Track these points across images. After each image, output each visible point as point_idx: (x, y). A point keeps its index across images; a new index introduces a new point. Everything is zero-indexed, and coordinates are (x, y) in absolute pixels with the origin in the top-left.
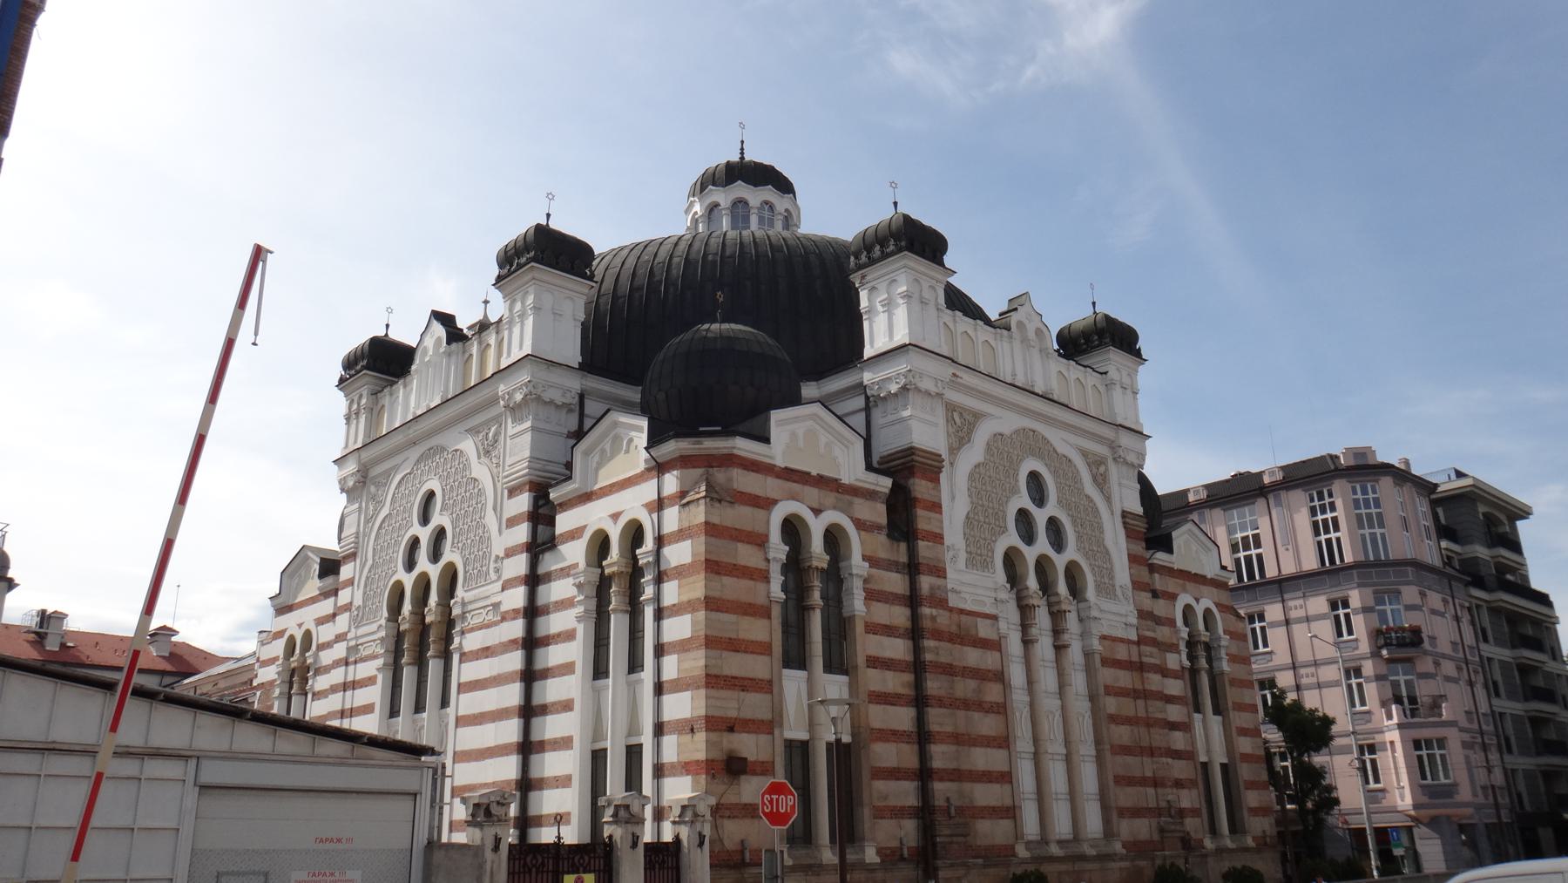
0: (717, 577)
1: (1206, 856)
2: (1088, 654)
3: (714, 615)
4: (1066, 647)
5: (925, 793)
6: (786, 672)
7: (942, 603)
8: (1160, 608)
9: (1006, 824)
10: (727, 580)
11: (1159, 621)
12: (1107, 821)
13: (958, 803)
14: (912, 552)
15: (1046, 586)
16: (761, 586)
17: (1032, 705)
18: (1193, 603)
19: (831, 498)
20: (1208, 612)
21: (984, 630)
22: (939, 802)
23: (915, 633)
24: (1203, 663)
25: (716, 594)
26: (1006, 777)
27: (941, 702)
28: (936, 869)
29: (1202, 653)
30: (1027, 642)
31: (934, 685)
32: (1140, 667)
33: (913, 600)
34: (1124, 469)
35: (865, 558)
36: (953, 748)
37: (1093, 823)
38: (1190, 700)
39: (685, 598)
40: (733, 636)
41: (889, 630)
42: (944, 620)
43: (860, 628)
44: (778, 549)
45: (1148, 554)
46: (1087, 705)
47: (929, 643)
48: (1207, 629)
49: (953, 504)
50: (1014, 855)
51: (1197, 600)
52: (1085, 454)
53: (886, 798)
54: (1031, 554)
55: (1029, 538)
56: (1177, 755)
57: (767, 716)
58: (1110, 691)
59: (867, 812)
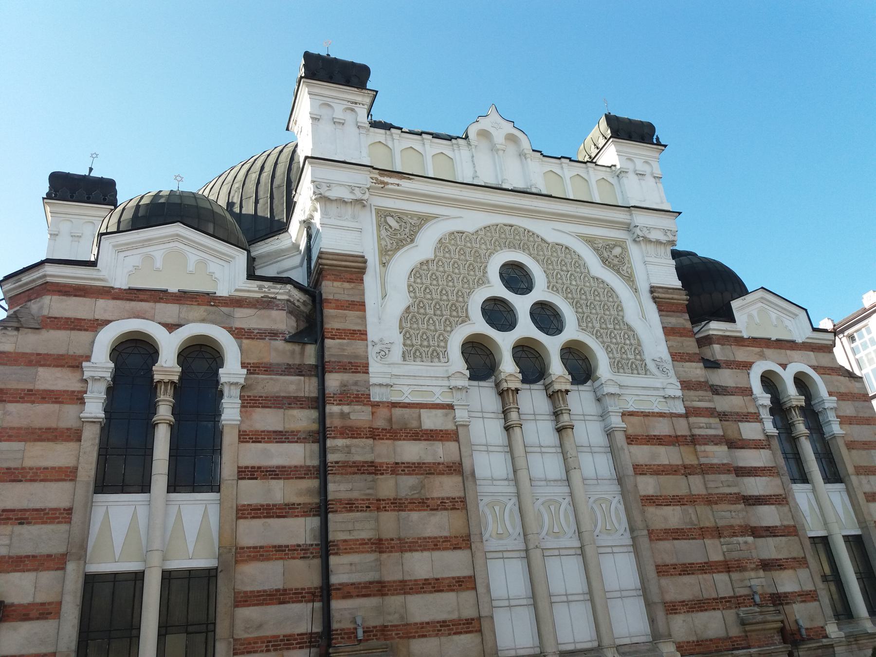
1: (832, 646)
2: (609, 433)
7: (362, 398)
8: (725, 377)
10: (12, 407)
11: (717, 390)
12: (652, 621)
13: (372, 623)
18: (778, 369)
19: (200, 311)
21: (431, 421)
24: (801, 428)
27: (350, 506)
31: (338, 488)
32: (693, 441)
34: (651, 248)
35: (243, 365)
36: (371, 557)
37: (630, 622)
40: (12, 465)
41: (281, 437)
42: (360, 415)
43: (229, 439)
45: (696, 329)
46: (615, 488)
49: (386, 303)
51: (784, 366)
52: (590, 241)
54: (505, 341)
56: (771, 532)
58: (640, 470)
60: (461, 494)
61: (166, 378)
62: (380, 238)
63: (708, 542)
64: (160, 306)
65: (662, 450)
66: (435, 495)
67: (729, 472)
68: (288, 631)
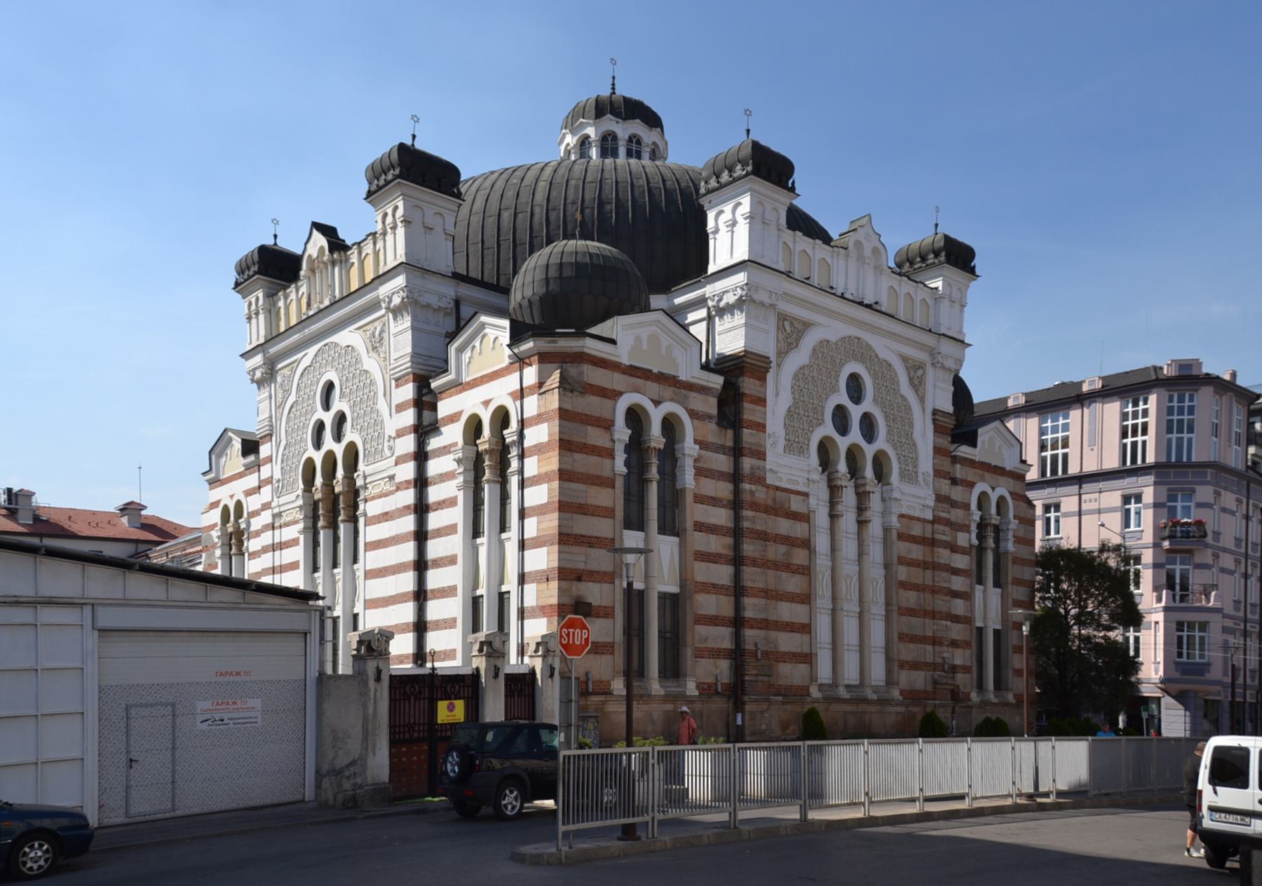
0: (569, 454)
2: (886, 530)
3: (566, 484)
4: (866, 522)
5: (738, 638)
6: (627, 533)
7: (760, 480)
8: (957, 493)
9: (803, 668)
10: (577, 456)
14: (737, 438)
15: (854, 470)
16: (607, 462)
17: (833, 569)
18: (989, 491)
20: (1001, 500)
21: (796, 505)
22: (749, 646)
23: (736, 505)
24: (990, 543)
25: (569, 467)
26: (806, 629)
27: (754, 563)
28: (743, 703)
29: (990, 534)
30: (833, 516)
31: (749, 548)
32: (932, 543)
33: (736, 477)
35: (696, 442)
36: (763, 601)
38: (974, 574)
39: (543, 470)
40: (582, 501)
42: (761, 494)
43: (689, 498)
44: (622, 433)
46: (882, 572)
47: (747, 513)
48: (998, 513)
49: (777, 401)
50: (808, 695)
51: (993, 489)
53: (706, 640)
54: (843, 443)
55: (843, 429)
57: (610, 568)
58: (902, 561)
59: (689, 652)
60: (806, 563)
61: (657, 446)
62: (778, 341)
63: (927, 621)
64: (649, 383)
65: (914, 547)
66: (795, 562)
67: (947, 571)
68: (719, 646)
